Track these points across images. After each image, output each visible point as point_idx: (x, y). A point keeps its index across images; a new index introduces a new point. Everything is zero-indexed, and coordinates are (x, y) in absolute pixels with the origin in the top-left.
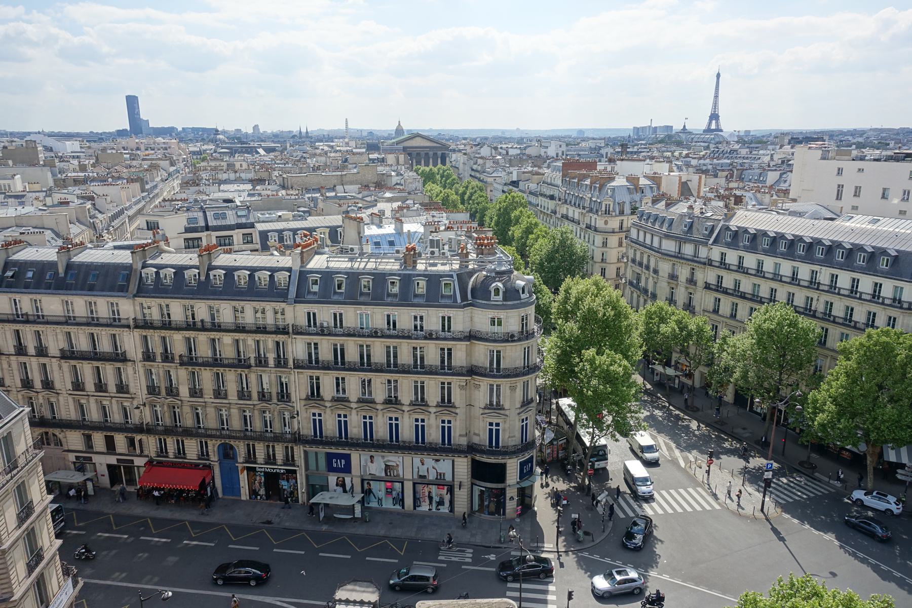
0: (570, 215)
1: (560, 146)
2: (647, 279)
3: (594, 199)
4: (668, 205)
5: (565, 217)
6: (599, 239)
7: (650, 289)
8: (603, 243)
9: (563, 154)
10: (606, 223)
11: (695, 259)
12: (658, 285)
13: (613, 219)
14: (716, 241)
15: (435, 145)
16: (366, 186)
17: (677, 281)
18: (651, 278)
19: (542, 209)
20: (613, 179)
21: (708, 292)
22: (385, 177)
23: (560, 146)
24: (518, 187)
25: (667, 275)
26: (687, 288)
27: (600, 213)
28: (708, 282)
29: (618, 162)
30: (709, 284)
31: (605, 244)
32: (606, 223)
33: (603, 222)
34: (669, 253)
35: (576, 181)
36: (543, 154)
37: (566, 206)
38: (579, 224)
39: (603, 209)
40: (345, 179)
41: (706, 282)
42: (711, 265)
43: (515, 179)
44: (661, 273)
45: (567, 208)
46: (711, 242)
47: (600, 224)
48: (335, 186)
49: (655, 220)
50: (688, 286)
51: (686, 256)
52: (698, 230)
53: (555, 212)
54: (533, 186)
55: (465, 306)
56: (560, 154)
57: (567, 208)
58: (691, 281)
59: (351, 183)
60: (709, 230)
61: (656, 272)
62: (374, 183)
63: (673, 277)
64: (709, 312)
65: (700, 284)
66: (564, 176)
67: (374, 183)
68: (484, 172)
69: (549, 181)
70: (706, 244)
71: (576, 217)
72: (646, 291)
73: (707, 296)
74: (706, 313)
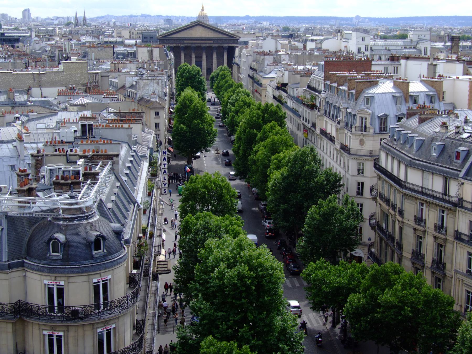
0: (329, 131)
1: (363, 39)
2: (394, 222)
3: (349, 111)
4: (422, 121)
5: (324, 133)
6: (353, 165)
7: (397, 237)
8: (359, 170)
9: (367, 49)
10: (362, 142)
11: (447, 198)
12: (404, 232)
13: (371, 138)
14: (467, 174)
15: (220, 36)
16: (71, 89)
17: (424, 226)
18: (397, 222)
19: (304, 122)
20: (375, 84)
21: (461, 244)
22: (99, 77)
23: (363, 39)
24: (285, 91)
25: (412, 218)
26: (435, 238)
27: (353, 129)
28: (460, 231)
29: (403, 62)
30: (461, 234)
31: (361, 172)
32: (362, 142)
33: (358, 141)
34: (414, 187)
35: (335, 85)
36: (343, 49)
37: (326, 119)
38: (334, 143)
39: (358, 123)
40: (44, 78)
41: (457, 231)
42: (462, 207)
43: (286, 82)
44: (406, 215)
45: (326, 122)
46: (461, 174)
47: (353, 144)
48: (30, 89)
49: (405, 142)
50: (437, 234)
51: (435, 194)
52: (450, 157)
53: (314, 125)
54: (299, 91)
55: (10, 267)
56: (363, 50)
57: (326, 122)
58: (440, 228)
59: (53, 85)
60: (462, 156)
61: (401, 213)
62: (83, 85)
63: (419, 220)
64: (462, 274)
65: (451, 231)
66: (326, 78)
67: (83, 85)
68: (262, 72)
69: (314, 86)
70: (456, 177)
71: (334, 134)
72: (393, 239)
73: (459, 249)
74: (458, 276)
